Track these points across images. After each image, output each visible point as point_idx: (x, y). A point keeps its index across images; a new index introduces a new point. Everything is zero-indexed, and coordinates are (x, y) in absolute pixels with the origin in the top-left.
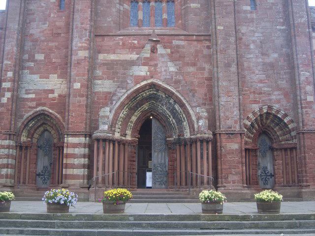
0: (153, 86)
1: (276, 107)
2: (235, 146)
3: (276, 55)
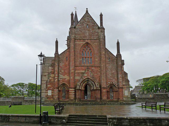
0: (88, 78)
1: (114, 83)
2: (105, 91)
3: (114, 71)
